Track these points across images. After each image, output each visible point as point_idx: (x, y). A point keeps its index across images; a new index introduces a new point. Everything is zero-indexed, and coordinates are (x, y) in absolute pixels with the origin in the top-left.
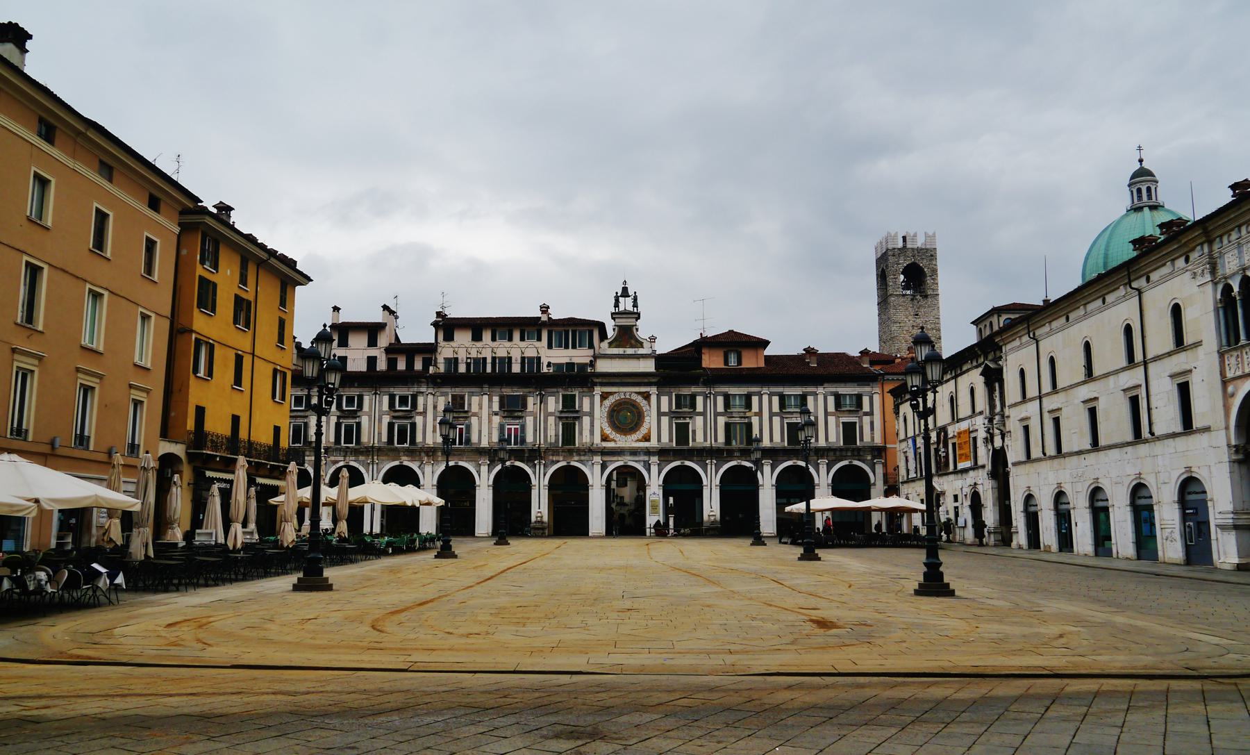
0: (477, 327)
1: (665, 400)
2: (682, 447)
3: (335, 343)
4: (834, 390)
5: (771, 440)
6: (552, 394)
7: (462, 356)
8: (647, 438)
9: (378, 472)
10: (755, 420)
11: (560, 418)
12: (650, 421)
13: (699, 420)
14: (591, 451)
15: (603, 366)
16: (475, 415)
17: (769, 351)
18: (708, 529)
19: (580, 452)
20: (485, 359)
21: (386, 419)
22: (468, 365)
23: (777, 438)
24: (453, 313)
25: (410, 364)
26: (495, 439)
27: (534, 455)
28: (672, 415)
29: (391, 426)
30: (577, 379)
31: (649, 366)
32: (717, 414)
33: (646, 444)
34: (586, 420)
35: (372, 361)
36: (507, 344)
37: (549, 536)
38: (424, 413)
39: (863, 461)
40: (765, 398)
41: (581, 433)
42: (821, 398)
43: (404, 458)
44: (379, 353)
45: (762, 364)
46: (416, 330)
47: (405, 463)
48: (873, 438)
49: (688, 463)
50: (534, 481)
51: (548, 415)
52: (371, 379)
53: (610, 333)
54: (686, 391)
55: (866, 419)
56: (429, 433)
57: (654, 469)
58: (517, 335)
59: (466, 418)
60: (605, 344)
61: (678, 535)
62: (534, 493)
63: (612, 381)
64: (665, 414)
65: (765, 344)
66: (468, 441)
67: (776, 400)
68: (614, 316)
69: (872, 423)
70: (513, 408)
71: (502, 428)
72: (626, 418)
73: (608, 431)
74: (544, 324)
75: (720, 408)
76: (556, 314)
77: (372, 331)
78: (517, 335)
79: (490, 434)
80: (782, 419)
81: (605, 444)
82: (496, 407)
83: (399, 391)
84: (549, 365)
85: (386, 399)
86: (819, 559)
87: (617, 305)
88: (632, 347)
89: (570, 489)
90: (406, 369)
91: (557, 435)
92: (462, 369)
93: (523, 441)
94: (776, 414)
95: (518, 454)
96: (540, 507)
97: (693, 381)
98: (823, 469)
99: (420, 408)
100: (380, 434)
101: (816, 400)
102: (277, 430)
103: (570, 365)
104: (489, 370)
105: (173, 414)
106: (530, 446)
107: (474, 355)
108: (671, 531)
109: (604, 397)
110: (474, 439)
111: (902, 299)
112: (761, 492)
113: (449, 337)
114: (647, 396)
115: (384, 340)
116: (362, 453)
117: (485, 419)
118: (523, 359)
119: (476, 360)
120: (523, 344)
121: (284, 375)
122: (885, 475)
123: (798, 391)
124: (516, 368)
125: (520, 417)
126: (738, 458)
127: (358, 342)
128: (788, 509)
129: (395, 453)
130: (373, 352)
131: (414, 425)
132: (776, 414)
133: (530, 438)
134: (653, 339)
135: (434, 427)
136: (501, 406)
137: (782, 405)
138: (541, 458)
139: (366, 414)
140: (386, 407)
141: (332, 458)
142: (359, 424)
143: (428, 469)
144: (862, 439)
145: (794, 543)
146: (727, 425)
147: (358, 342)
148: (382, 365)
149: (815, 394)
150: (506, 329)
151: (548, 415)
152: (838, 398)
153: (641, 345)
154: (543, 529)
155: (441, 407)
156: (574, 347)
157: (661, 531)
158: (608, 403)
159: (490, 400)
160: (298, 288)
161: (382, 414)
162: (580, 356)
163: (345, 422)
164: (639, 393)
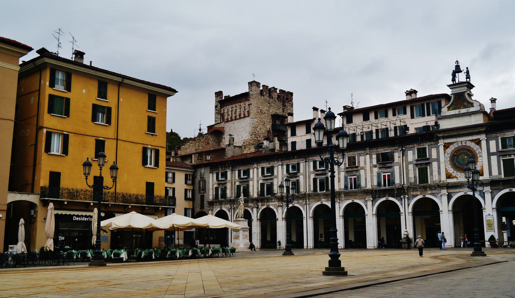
0: (365, 113)
1: (493, 143)
7: (359, 132)
9: (310, 209)
11: (417, 165)
14: (439, 186)
15: (444, 125)
16: (362, 168)
21: (313, 176)
22: (362, 137)
24: (356, 107)
26: (375, 183)
27: (401, 192)
28: (499, 154)
29: (315, 180)
30: (429, 135)
34: (435, 164)
41: (432, 174)
47: (324, 203)
50: (402, 210)
52: (309, 152)
57: (488, 196)
58: (390, 113)
63: (455, 133)
64: (493, 154)
66: (359, 185)
70: (385, 161)
71: (379, 175)
72: (464, 160)
73: (451, 170)
76: (419, 95)
77: (307, 124)
78: (390, 113)
81: (450, 181)
82: (375, 162)
85: (312, 164)
87: (454, 80)
88: (465, 107)
89: (427, 213)
91: (415, 177)
92: (359, 139)
93: (394, 183)
100: (309, 186)
102: (150, 186)
103: (427, 128)
104: (374, 137)
105: (36, 178)
106: (397, 186)
107: (366, 130)
109: (446, 146)
110: (363, 184)
113: (349, 121)
114: (478, 142)
116: (300, 198)
120: (394, 118)
121: (157, 152)
125: (390, 167)
127: (301, 131)
130: (308, 137)
133: (397, 181)
136: (378, 161)
138: (405, 194)
140: (312, 169)
142: (298, 181)
147: (301, 131)
156: (429, 115)
158: (449, 150)
159: (371, 158)
160: (168, 99)
162: (430, 120)
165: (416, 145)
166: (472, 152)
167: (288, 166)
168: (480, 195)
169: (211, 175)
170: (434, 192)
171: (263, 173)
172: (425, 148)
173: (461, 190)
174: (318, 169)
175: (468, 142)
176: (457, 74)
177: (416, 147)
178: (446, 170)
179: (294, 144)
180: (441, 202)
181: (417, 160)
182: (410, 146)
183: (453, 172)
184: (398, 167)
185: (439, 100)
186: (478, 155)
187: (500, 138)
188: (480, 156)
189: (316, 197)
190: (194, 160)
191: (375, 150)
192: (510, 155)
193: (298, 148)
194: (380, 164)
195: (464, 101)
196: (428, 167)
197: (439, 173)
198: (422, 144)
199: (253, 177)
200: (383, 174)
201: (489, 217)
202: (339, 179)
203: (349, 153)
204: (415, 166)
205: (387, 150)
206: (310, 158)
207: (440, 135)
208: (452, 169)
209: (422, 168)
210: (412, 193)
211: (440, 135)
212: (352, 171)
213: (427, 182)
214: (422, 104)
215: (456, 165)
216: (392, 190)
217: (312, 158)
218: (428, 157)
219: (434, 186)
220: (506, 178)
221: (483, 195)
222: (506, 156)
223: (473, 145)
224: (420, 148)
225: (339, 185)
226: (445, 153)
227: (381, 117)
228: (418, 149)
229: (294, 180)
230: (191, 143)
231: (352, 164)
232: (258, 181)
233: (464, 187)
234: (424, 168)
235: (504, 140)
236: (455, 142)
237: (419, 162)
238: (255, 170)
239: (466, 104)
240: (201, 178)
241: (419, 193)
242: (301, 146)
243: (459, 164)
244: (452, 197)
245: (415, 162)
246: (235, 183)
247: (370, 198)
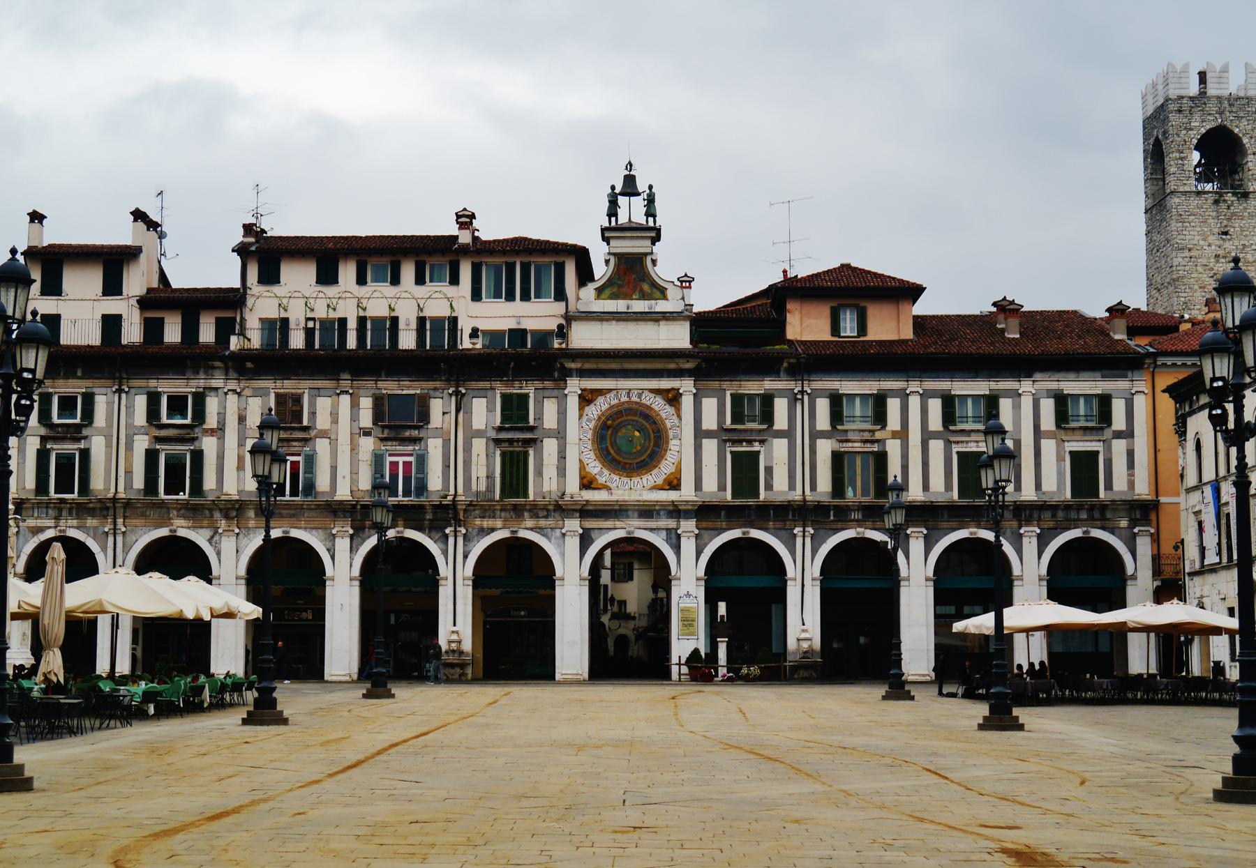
0: (326, 256)
1: (710, 405)
2: (745, 501)
3: (36, 288)
4: (1054, 386)
5: (926, 487)
6: (481, 393)
7: (297, 315)
8: (673, 483)
9: (126, 550)
10: (893, 448)
11: (497, 442)
12: (680, 449)
13: (779, 447)
14: (560, 509)
15: (584, 337)
16: (324, 434)
17: (922, 307)
18: (796, 668)
19: (537, 510)
20: (343, 322)
21: (142, 444)
22: (309, 333)
23: (937, 483)
24: (278, 226)
25: (190, 330)
26: (365, 483)
27: (444, 516)
28: (725, 435)
29: (151, 456)
31: (678, 337)
32: (815, 435)
33: (672, 496)
34: (550, 446)
35: (111, 324)
36: (387, 289)
37: (475, 680)
38: (219, 431)
39: (1112, 531)
40: (914, 402)
41: (539, 473)
42: (1027, 403)
43: (178, 522)
44: (126, 308)
45: (908, 333)
46: (204, 264)
47: (182, 533)
48: (1131, 485)
49: (756, 534)
50: (444, 570)
51: (472, 434)
52: (110, 361)
53: (600, 270)
54: (753, 387)
55: (1119, 446)
56: (229, 471)
57: (688, 545)
58: (408, 272)
59: (306, 440)
60: (589, 291)
61: (736, 677)
62: (445, 593)
63: (603, 365)
64: (709, 434)
65: (914, 292)
66: (310, 487)
67: (935, 406)
68: (607, 234)
69: (1130, 454)
70: (400, 421)
71: (378, 460)
72: (630, 441)
73: (595, 467)
74: (465, 251)
75: (823, 422)
76: (489, 230)
77: (113, 263)
78: (408, 272)
79: (354, 473)
80: (948, 443)
82: (366, 419)
83: (168, 387)
84: (474, 333)
85: (141, 402)
86: (1021, 727)
88: (644, 297)
89: (516, 584)
90: (181, 341)
91: (490, 477)
92: (297, 341)
93: (422, 488)
94: (936, 435)
95: (410, 515)
96: (456, 623)
97: (768, 367)
98: (1030, 545)
99: (211, 421)
100: (129, 473)
101: (1017, 407)
103: (518, 335)
104: (352, 343)
106: (435, 499)
107: (321, 312)
108: (722, 671)
109: (586, 398)
110: (322, 483)
111: (1194, 201)
112: (904, 592)
113: (270, 276)
114: (673, 398)
116: (92, 512)
117: (343, 444)
118: (421, 321)
119: (326, 324)
122: (1156, 559)
123: (981, 387)
124: (407, 341)
125: (415, 440)
126: (859, 523)
127: (82, 285)
128: (958, 626)
129: (161, 512)
130: (113, 306)
131: (198, 456)
132: (936, 435)
133: (435, 483)
134: (686, 282)
135: (241, 459)
136: (378, 416)
137: (949, 417)
138: (458, 523)
139: (100, 432)
140: (140, 418)
141: (31, 522)
142: (85, 454)
143: (228, 544)
144: (1109, 486)
145: (970, 695)
146: (838, 459)
147: (82, 285)
148: (132, 333)
149: (1016, 395)
150: (386, 260)
151: (472, 434)
152: (1061, 401)
153: (662, 293)
154: (463, 666)
155: (254, 420)
156: (525, 297)
157: (701, 669)
158: (594, 411)
159: (355, 405)
162: (538, 315)
163: (57, 448)
164: (657, 392)
165: (497, 384)
166: (655, 422)
168: (668, 540)
170: (542, 523)
172: (526, 396)
173: (618, 524)
174: (165, 420)
175: (646, 393)
176: (622, 200)
177: (500, 389)
178: (582, 467)
180: (563, 555)
181: (500, 429)
182: (482, 384)
183: (601, 473)
184: (439, 442)
185: (559, 259)
186: (671, 433)
187: (728, 393)
188: (675, 437)
191: (371, 384)
192: (750, 442)
194: (383, 427)
195: (643, 280)
196: (531, 452)
197: (562, 471)
198: (517, 384)
200: (389, 459)
201: (688, 600)
203: (279, 383)
204: (492, 444)
205: (408, 388)
207: (573, 365)
208: (597, 463)
209: (512, 452)
210: (478, 522)
211: (573, 365)
212: (288, 440)
213: (526, 495)
214: (507, 264)
215: (609, 453)
216: (420, 508)
217: (142, 383)
218: (532, 422)
219: (545, 508)
220: (738, 502)
221: (674, 541)
222: (740, 442)
223: (658, 404)
224: (511, 395)
226: (581, 416)
227: (376, 279)
228: (504, 396)
231: (288, 417)
233: (628, 517)
234: (519, 453)
235: (737, 400)
236: (611, 390)
237: (504, 435)
239: (646, 287)
241: (499, 523)
243: (618, 451)
244: (591, 541)
245: (493, 434)
247: (343, 529)
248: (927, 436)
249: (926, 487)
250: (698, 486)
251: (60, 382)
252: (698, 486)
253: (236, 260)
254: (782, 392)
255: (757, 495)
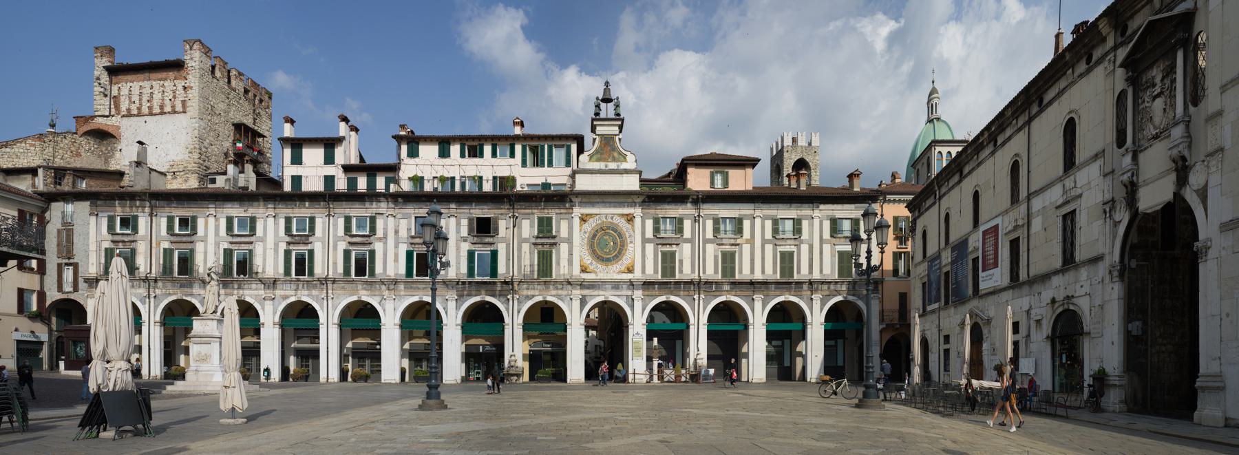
5: (763, 272)
6: (527, 216)
8: (630, 270)
11: (535, 244)
12: (634, 251)
13: (687, 247)
20: (453, 178)
21: (342, 246)
29: (347, 254)
32: (706, 241)
33: (630, 276)
34: (564, 247)
35: (329, 180)
38: (384, 238)
41: (558, 264)
44: (336, 171)
52: (328, 197)
58: (488, 149)
67: (769, 224)
72: (607, 245)
73: (588, 260)
74: (517, 138)
75: (710, 234)
78: (488, 149)
81: (585, 276)
82: (464, 232)
85: (341, 222)
91: (531, 266)
94: (768, 242)
99: (380, 233)
100: (335, 264)
101: (811, 225)
103: (546, 185)
104: (458, 188)
109: (583, 219)
113: (413, 153)
115: (340, 155)
118: (495, 178)
125: (491, 244)
127: (312, 156)
130: (329, 170)
131: (372, 253)
132: (768, 242)
133: (501, 269)
135: (396, 255)
137: (775, 231)
138: (514, 291)
139: (319, 240)
140: (341, 231)
142: (311, 252)
147: (312, 156)
148: (341, 185)
152: (835, 223)
155: (403, 233)
156: (550, 164)
159: (458, 224)
161: (337, 239)
162: (555, 175)
167: (288, 221)
169: (93, 219)
171: (229, 228)
174: (354, 232)
179: (297, 180)
189: (347, 286)
190: (41, 183)
193: (306, 187)
197: (570, 262)
199: (206, 235)
202: (396, 255)
206: (337, 211)
216: (494, 283)
217: (342, 211)
219: (561, 283)
223: (622, 224)
225: (396, 268)
229: (302, 248)
230: (31, 145)
232: (217, 244)
237: (539, 241)
238: (211, 220)
240: (64, 224)
242: (314, 184)
245: (533, 240)
246: (158, 244)
248: (764, 242)
249: (763, 272)
250: (643, 271)
251: (297, 210)
252: (643, 271)
253: (395, 142)
254: (688, 217)
255: (673, 275)
